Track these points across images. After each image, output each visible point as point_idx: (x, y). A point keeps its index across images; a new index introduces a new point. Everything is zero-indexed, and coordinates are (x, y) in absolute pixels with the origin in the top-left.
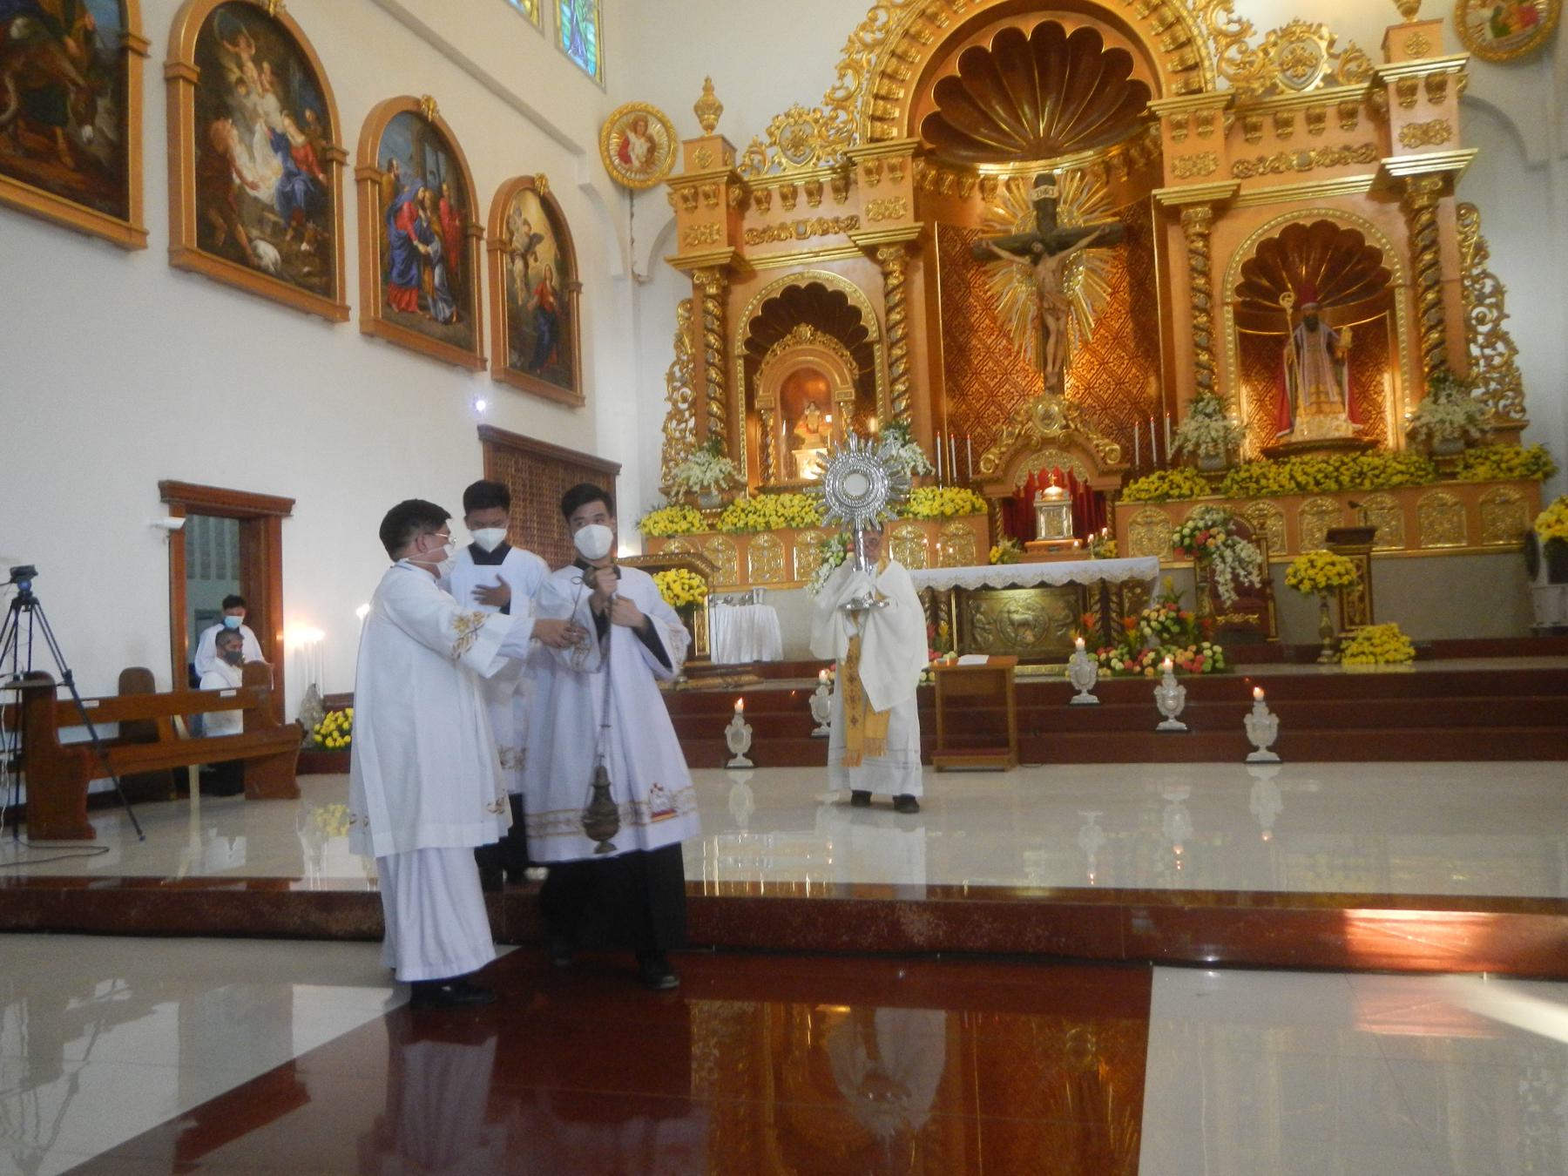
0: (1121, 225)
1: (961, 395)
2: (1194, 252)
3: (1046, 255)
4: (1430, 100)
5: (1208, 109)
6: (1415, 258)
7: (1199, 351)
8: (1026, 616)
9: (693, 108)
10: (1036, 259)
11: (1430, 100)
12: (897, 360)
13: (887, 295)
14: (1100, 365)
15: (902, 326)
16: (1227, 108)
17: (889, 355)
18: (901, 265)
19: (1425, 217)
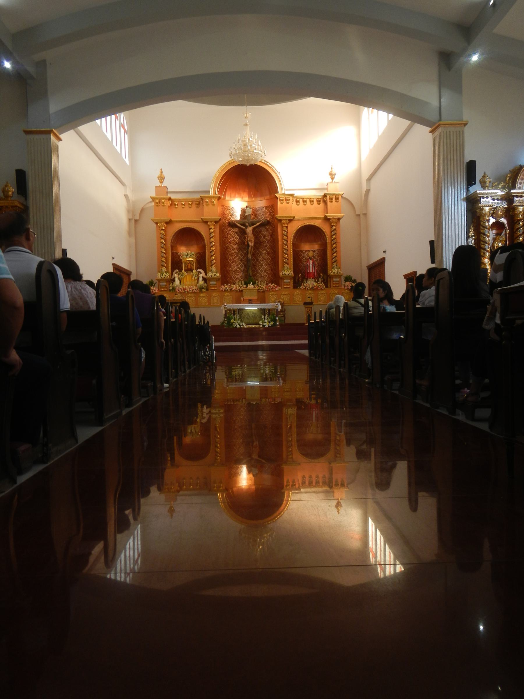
2: (285, 231)
3: (249, 227)
4: (336, 201)
5: (289, 197)
6: (332, 236)
9: (157, 176)
10: (246, 227)
12: (213, 251)
14: (261, 254)
16: (293, 197)
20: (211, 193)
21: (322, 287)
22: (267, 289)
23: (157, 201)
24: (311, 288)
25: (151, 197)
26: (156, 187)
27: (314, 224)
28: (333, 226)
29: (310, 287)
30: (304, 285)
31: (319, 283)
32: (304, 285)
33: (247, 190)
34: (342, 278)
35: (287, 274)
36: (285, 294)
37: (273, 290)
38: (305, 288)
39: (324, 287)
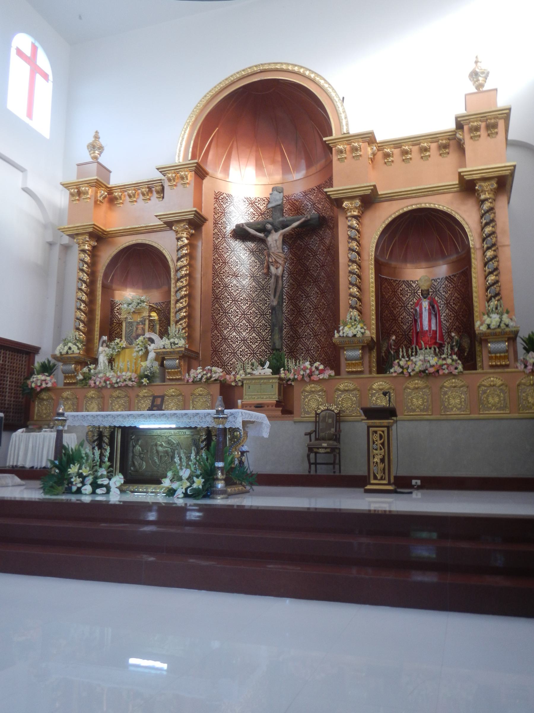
0: (317, 216)
1: (224, 313)
2: (350, 227)
3: (273, 231)
4: (489, 135)
7: (351, 286)
8: (166, 449)
9: (86, 147)
10: (267, 232)
11: (489, 135)
12: (181, 289)
13: (178, 251)
14: (306, 297)
15: (185, 269)
17: (176, 286)
18: (186, 234)
19: (486, 206)
20: (179, 159)
21: (452, 368)
22: (296, 377)
23: (72, 191)
24: (420, 371)
25: (63, 185)
26: (78, 165)
27: (432, 206)
28: (483, 201)
29: (417, 369)
30: (399, 365)
31: (443, 356)
32: (399, 365)
33: (279, 158)
34: (519, 340)
35: (350, 335)
36: (347, 391)
37: (312, 378)
38: (402, 372)
39: (460, 367)
